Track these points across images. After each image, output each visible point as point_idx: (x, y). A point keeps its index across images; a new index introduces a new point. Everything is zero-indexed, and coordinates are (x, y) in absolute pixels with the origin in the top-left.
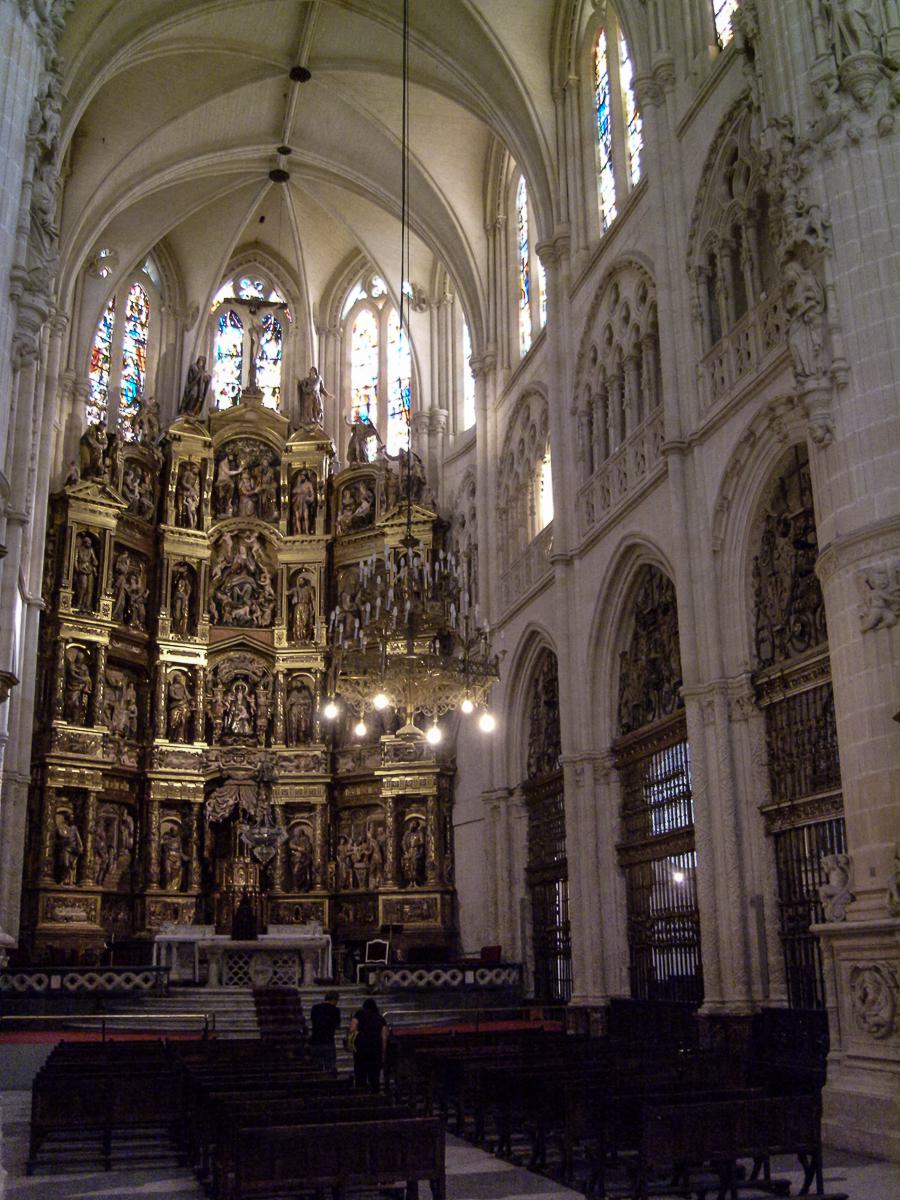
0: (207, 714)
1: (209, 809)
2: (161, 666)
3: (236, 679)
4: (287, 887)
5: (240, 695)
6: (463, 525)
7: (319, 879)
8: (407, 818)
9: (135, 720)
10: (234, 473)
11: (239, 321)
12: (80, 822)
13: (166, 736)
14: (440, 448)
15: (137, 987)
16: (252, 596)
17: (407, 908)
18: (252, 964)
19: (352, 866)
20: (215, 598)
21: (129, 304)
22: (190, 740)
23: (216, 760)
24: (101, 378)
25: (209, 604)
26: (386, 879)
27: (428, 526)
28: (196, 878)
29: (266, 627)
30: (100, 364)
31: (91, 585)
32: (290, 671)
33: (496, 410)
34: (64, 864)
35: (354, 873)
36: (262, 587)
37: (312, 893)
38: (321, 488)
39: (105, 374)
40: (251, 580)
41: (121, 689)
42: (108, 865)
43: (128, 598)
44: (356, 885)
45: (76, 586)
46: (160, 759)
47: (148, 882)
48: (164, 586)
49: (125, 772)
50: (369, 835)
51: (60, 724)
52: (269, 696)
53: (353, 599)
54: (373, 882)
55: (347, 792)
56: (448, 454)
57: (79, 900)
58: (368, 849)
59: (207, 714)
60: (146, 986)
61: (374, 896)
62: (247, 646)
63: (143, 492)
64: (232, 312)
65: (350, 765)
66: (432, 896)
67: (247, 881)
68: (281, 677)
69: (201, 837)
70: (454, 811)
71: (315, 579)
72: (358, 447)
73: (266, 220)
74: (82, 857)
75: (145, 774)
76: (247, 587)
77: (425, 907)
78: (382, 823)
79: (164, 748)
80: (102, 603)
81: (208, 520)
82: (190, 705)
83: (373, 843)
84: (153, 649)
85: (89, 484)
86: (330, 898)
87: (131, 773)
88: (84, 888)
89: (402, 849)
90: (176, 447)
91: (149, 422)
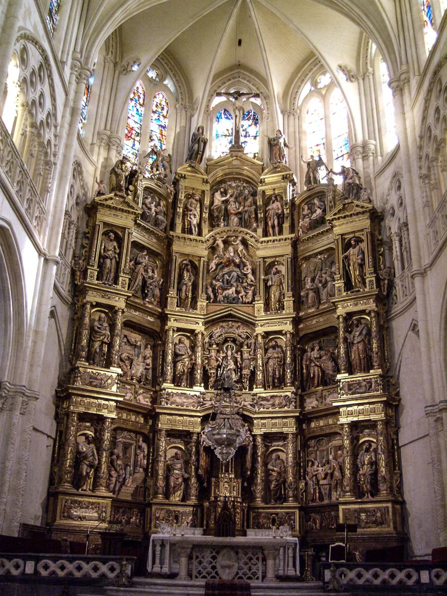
0: (204, 368)
2: (168, 330)
3: (226, 341)
4: (265, 500)
5: (229, 353)
6: (393, 215)
7: (291, 494)
8: (361, 441)
9: (150, 371)
10: (224, 199)
11: (230, 115)
12: (97, 441)
13: (173, 382)
14: (371, 167)
15: (103, 576)
16: (237, 280)
17: (363, 516)
18: (219, 558)
19: (318, 481)
20: (211, 284)
21: (155, 103)
22: (191, 384)
23: (210, 400)
24: (134, 145)
25: (207, 288)
26: (345, 492)
27: (367, 215)
28: (193, 491)
30: (133, 136)
32: (267, 334)
33: (412, 108)
34: (82, 474)
35: (320, 489)
36: (246, 275)
37: (285, 504)
38: (286, 204)
39: (137, 143)
40: (238, 270)
42: (125, 479)
43: (144, 281)
44: (321, 498)
45: (101, 266)
46: (166, 398)
48: (173, 275)
50: (331, 457)
51: (82, 364)
52: (252, 353)
53: (313, 280)
54: (334, 496)
55: (313, 425)
56: (377, 169)
57: (93, 504)
58: (330, 469)
59: (204, 368)
60: (111, 575)
61: (335, 507)
62: (235, 317)
63: (158, 210)
64: (225, 110)
65: (315, 403)
66: (384, 505)
67: (230, 493)
68: (260, 338)
69: (198, 460)
71: (283, 269)
72: (311, 175)
73: (243, 43)
74: (97, 469)
75: (154, 409)
76: (234, 274)
77: (379, 514)
78: (341, 447)
79: (170, 391)
80: (121, 279)
81: (205, 228)
82: (191, 360)
83: (334, 463)
84: (163, 318)
85: (112, 195)
87: (145, 409)
88: (98, 493)
90: (183, 183)
91: (163, 166)
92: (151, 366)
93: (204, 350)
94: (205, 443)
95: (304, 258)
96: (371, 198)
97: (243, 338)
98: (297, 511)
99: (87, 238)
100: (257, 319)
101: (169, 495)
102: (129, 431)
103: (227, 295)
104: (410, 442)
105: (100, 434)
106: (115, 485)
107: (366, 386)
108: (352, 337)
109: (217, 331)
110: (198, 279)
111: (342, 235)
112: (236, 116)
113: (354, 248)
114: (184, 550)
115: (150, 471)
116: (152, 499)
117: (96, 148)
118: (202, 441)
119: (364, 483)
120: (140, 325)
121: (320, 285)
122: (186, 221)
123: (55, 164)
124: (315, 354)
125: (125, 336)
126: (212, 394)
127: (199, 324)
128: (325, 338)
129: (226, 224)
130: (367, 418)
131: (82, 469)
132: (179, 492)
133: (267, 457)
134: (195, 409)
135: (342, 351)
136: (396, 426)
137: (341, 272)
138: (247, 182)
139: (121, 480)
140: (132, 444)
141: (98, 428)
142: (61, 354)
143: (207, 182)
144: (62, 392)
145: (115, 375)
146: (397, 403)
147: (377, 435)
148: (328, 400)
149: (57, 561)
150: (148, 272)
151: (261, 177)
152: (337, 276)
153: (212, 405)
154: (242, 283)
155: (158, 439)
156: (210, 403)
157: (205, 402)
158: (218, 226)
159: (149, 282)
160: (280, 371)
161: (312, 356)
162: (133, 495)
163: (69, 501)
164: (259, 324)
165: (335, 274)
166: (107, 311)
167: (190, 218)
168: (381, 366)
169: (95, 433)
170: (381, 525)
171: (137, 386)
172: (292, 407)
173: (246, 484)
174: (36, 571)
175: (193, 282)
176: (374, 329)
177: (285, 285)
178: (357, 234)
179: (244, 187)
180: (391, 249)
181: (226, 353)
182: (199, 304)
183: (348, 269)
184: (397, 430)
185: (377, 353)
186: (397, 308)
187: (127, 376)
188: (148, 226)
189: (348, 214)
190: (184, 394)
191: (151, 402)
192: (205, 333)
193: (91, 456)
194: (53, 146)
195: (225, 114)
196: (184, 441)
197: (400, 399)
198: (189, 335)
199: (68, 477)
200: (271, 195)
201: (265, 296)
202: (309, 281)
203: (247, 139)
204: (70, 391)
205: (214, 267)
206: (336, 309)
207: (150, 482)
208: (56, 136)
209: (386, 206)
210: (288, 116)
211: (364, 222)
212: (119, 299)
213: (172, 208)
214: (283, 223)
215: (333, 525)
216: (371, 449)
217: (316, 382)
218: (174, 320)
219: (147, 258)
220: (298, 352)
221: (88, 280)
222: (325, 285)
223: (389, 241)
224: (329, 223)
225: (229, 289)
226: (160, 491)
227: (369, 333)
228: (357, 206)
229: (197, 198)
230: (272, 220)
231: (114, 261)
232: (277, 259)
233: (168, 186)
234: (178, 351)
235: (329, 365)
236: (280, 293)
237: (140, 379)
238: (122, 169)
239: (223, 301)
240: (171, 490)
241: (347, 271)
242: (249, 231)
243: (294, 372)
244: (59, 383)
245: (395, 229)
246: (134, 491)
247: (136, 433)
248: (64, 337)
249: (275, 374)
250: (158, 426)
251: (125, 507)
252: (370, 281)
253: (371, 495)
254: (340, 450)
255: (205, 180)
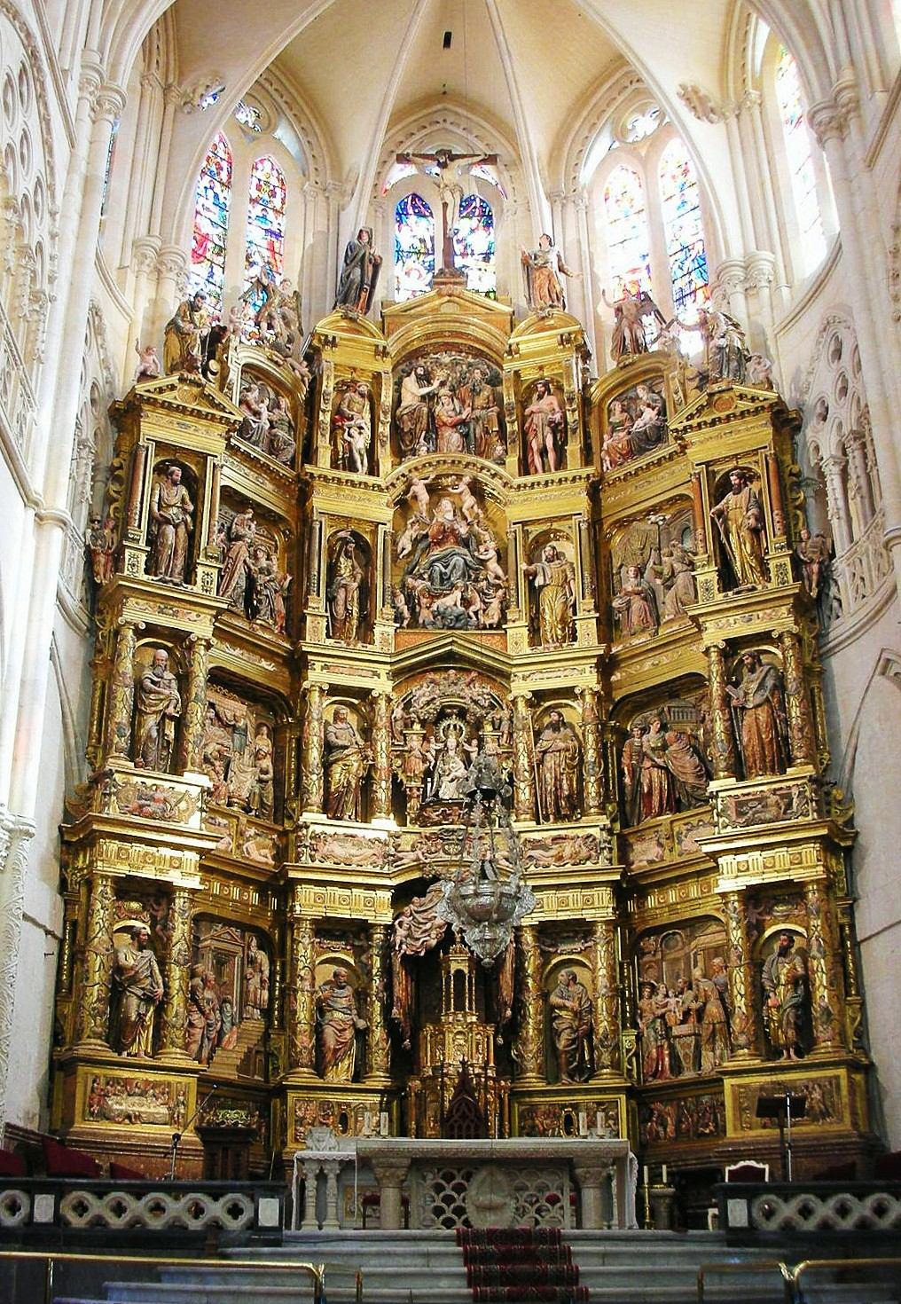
0: (395, 776)
1: (401, 932)
3: (442, 715)
5: (452, 742)
7: (606, 1059)
8: (767, 933)
13: (325, 808)
14: (767, 309)
15: (216, 1227)
18: (472, 1191)
19: (668, 1029)
20: (403, 586)
22: (366, 812)
25: (394, 595)
28: (380, 1058)
29: (491, 627)
31: (182, 544)
32: (539, 696)
35: (671, 1047)
36: (483, 562)
37: (593, 1083)
38: (571, 400)
40: (466, 551)
41: (245, 730)
42: (221, 1033)
43: (251, 579)
44: (676, 1067)
47: (294, 1064)
49: (247, 867)
50: (697, 973)
51: (118, 763)
52: (503, 741)
53: (640, 572)
55: (651, 901)
57: (155, 1085)
58: (696, 998)
59: (395, 776)
60: (234, 1225)
62: (462, 658)
63: (275, 418)
68: (521, 705)
69: (388, 987)
70: (857, 915)
71: (569, 550)
72: (627, 334)
74: (161, 1007)
75: (284, 872)
76: (459, 560)
78: (718, 951)
79: (318, 829)
80: (200, 570)
81: (385, 457)
83: (705, 985)
84: (296, 664)
85: (174, 379)
86: (630, 1092)
88: (165, 1061)
89: (763, 989)
90: (328, 355)
91: (284, 317)
92: (271, 775)
93: (393, 737)
94: (404, 946)
95: (616, 522)
96: (771, 377)
97: (483, 707)
98: (623, 1097)
99: (117, 479)
100: (515, 662)
101: (326, 1068)
102: (228, 923)
103: (442, 610)
104: (885, 929)
105: (165, 928)
106: (201, 1047)
107: (777, 804)
108: (742, 694)
109: (422, 692)
110: (373, 575)
111: (708, 464)
112: (445, 205)
113: (738, 492)
114: (393, 1170)
115: (278, 1014)
116: (285, 1078)
117: (131, 277)
118: (398, 942)
119: (780, 1026)
120: (245, 678)
121: (659, 581)
122: (340, 442)
123: (52, 299)
124: (652, 739)
125: (212, 705)
126: (413, 836)
127: (379, 676)
128: (673, 704)
129: (432, 448)
130: (783, 877)
131: (127, 1008)
132: (346, 1062)
133: (547, 978)
134: (377, 870)
135: (719, 727)
136: (847, 895)
137: (710, 546)
138: (479, 354)
139: (213, 1034)
140: (234, 954)
141: (160, 915)
142: (68, 746)
143: (385, 353)
144: (74, 831)
145: (195, 792)
146: (849, 843)
147: (807, 915)
148: (688, 844)
149: (106, 1193)
150: (256, 558)
151: (511, 341)
152: (700, 559)
153: (418, 859)
154: (476, 580)
155: (293, 940)
156: (412, 856)
157: (400, 855)
158: (414, 452)
159: (260, 582)
160: (571, 780)
161: (645, 744)
162: (239, 1069)
163: (103, 1080)
164: (520, 675)
165: (695, 554)
166: (170, 645)
167: (349, 435)
168: (810, 758)
169: (152, 927)
170: (824, 1118)
171: (243, 820)
172: (602, 863)
173: (500, 1041)
174: (58, 1217)
175: (362, 580)
176: (792, 674)
177: (576, 586)
178: (742, 463)
179: (470, 365)
180: (821, 495)
181: (445, 742)
182: (377, 630)
183: (724, 541)
184: (852, 905)
185: (801, 730)
186: (838, 629)
187: (218, 797)
188: (257, 452)
189: (723, 415)
190: (351, 836)
191: (274, 858)
192: (394, 696)
193: (146, 977)
194: (47, 258)
195: (414, 207)
196: (352, 945)
197: (857, 833)
198: (356, 702)
199: (95, 1024)
200: (535, 382)
201: (531, 609)
202: (631, 574)
203: (469, 261)
204: (95, 827)
205: (409, 548)
206: (700, 631)
207: (278, 1042)
208: (53, 236)
209: (806, 397)
210: (563, 206)
211: (760, 433)
212: (198, 616)
213: (305, 414)
214: (565, 443)
215: (707, 1126)
216: (793, 950)
217: (656, 799)
218: (322, 668)
219: (253, 526)
220: (611, 738)
221: (126, 573)
222: (669, 584)
223: (816, 477)
224: (676, 438)
225: (445, 595)
226: (305, 1058)
227: (780, 685)
228: (741, 397)
229: (364, 389)
230: (540, 435)
231: (182, 529)
232: (555, 526)
233: (296, 365)
234: (333, 738)
235: (685, 765)
236: (565, 603)
237: (248, 803)
238: (192, 321)
239: (434, 623)
240: (329, 1056)
241: (722, 547)
242: (487, 463)
243: (603, 782)
244: (66, 812)
245: (829, 448)
246: (242, 1061)
247: (244, 927)
248: (74, 707)
249: (561, 786)
250: (292, 909)
251: (225, 1097)
252: (779, 566)
253: (796, 1053)
254: (716, 956)
255: (381, 349)
